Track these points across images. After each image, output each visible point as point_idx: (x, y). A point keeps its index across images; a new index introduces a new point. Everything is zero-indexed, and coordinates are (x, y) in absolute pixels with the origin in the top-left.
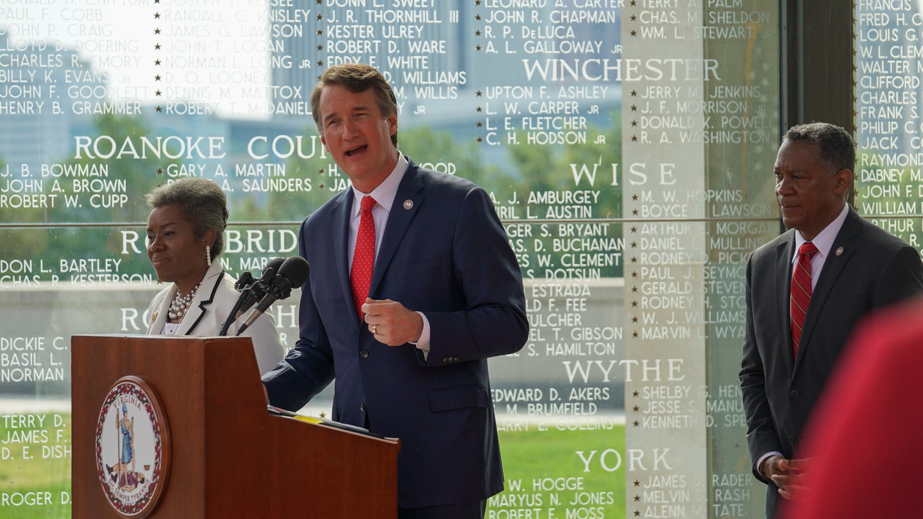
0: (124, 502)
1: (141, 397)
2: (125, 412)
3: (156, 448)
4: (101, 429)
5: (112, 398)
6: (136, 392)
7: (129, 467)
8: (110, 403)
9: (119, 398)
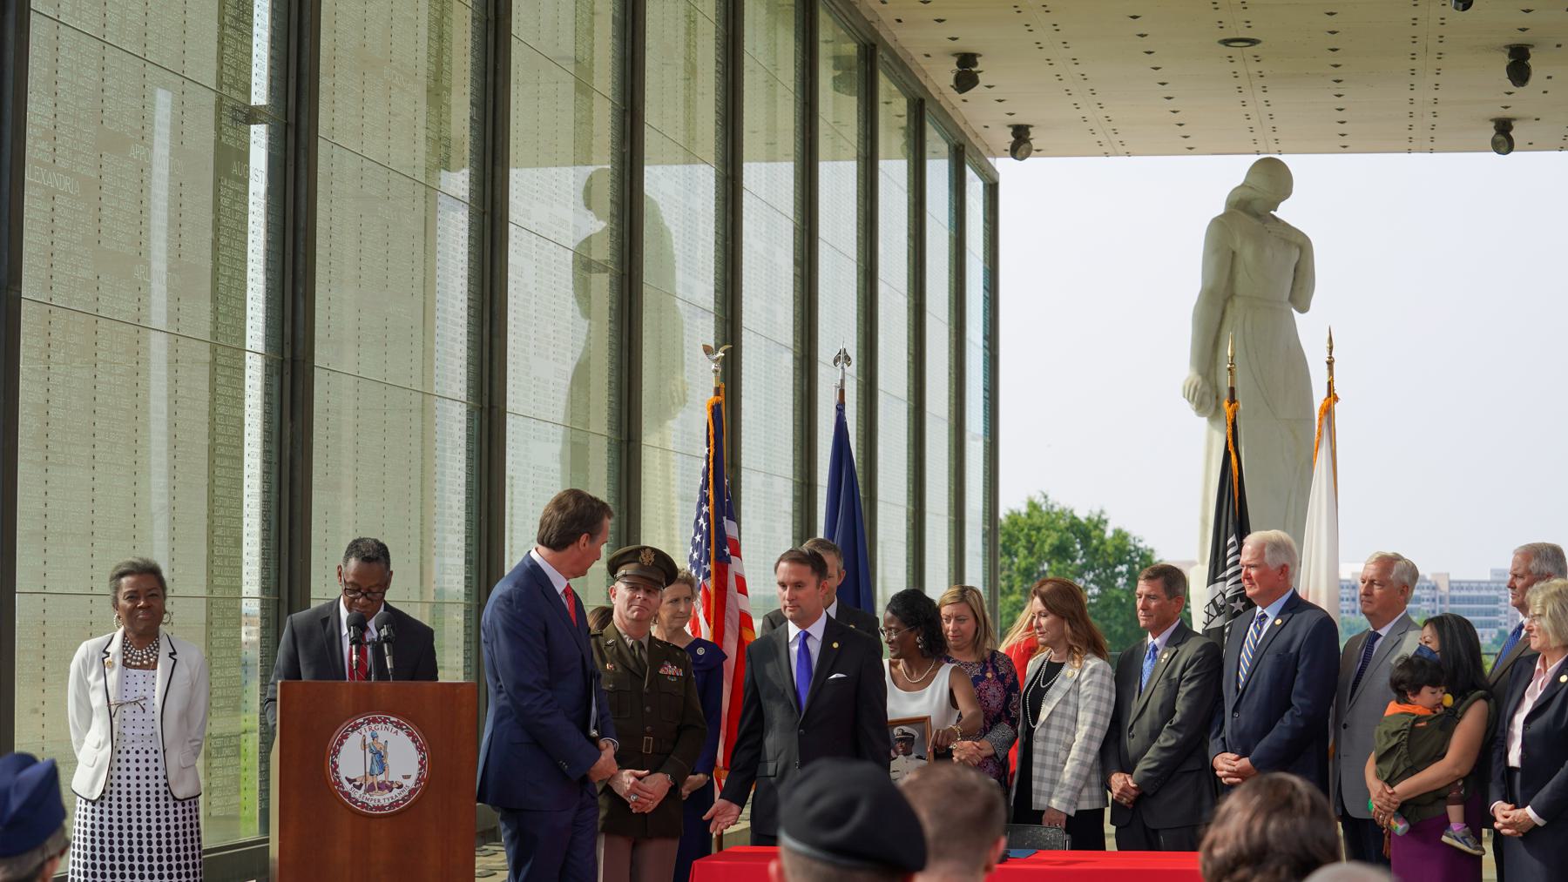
0: (371, 804)
1: (398, 726)
2: (374, 737)
3: (420, 763)
4: (336, 753)
5: (356, 727)
6: (391, 722)
7: (381, 778)
8: (352, 731)
9: (367, 729)
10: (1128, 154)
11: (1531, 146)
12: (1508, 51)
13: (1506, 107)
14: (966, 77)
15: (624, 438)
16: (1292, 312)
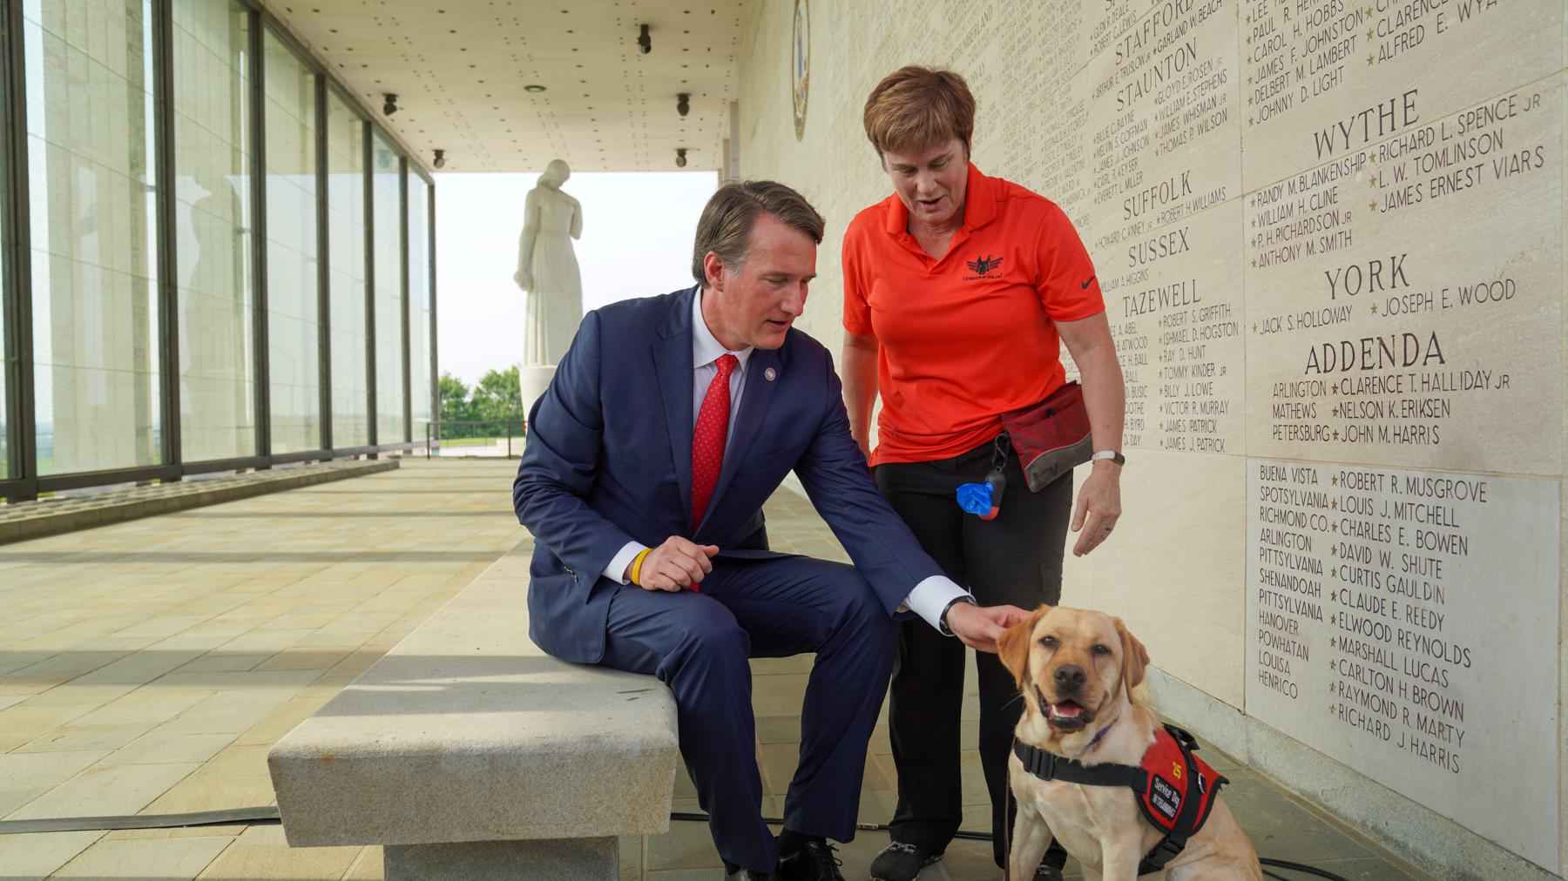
10: (499, 171)
11: (697, 168)
12: (678, 98)
13: (682, 141)
14: (390, 108)
15: (13, 241)
16: (570, 241)
